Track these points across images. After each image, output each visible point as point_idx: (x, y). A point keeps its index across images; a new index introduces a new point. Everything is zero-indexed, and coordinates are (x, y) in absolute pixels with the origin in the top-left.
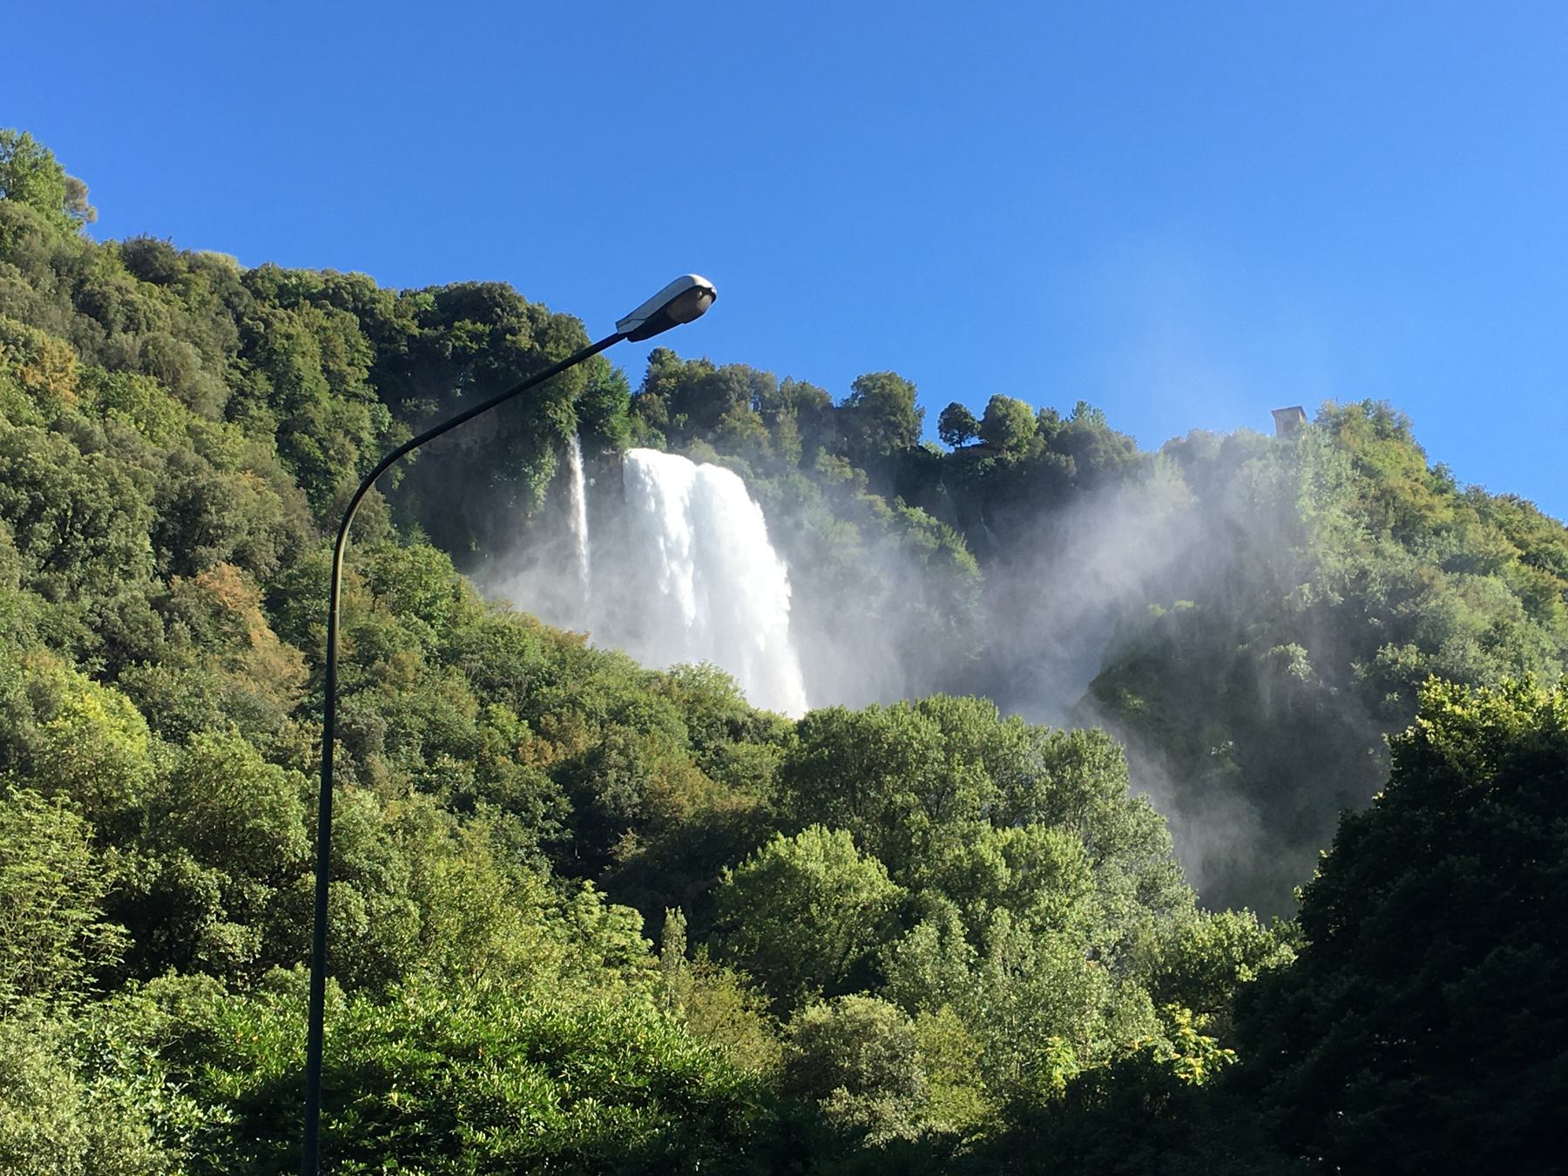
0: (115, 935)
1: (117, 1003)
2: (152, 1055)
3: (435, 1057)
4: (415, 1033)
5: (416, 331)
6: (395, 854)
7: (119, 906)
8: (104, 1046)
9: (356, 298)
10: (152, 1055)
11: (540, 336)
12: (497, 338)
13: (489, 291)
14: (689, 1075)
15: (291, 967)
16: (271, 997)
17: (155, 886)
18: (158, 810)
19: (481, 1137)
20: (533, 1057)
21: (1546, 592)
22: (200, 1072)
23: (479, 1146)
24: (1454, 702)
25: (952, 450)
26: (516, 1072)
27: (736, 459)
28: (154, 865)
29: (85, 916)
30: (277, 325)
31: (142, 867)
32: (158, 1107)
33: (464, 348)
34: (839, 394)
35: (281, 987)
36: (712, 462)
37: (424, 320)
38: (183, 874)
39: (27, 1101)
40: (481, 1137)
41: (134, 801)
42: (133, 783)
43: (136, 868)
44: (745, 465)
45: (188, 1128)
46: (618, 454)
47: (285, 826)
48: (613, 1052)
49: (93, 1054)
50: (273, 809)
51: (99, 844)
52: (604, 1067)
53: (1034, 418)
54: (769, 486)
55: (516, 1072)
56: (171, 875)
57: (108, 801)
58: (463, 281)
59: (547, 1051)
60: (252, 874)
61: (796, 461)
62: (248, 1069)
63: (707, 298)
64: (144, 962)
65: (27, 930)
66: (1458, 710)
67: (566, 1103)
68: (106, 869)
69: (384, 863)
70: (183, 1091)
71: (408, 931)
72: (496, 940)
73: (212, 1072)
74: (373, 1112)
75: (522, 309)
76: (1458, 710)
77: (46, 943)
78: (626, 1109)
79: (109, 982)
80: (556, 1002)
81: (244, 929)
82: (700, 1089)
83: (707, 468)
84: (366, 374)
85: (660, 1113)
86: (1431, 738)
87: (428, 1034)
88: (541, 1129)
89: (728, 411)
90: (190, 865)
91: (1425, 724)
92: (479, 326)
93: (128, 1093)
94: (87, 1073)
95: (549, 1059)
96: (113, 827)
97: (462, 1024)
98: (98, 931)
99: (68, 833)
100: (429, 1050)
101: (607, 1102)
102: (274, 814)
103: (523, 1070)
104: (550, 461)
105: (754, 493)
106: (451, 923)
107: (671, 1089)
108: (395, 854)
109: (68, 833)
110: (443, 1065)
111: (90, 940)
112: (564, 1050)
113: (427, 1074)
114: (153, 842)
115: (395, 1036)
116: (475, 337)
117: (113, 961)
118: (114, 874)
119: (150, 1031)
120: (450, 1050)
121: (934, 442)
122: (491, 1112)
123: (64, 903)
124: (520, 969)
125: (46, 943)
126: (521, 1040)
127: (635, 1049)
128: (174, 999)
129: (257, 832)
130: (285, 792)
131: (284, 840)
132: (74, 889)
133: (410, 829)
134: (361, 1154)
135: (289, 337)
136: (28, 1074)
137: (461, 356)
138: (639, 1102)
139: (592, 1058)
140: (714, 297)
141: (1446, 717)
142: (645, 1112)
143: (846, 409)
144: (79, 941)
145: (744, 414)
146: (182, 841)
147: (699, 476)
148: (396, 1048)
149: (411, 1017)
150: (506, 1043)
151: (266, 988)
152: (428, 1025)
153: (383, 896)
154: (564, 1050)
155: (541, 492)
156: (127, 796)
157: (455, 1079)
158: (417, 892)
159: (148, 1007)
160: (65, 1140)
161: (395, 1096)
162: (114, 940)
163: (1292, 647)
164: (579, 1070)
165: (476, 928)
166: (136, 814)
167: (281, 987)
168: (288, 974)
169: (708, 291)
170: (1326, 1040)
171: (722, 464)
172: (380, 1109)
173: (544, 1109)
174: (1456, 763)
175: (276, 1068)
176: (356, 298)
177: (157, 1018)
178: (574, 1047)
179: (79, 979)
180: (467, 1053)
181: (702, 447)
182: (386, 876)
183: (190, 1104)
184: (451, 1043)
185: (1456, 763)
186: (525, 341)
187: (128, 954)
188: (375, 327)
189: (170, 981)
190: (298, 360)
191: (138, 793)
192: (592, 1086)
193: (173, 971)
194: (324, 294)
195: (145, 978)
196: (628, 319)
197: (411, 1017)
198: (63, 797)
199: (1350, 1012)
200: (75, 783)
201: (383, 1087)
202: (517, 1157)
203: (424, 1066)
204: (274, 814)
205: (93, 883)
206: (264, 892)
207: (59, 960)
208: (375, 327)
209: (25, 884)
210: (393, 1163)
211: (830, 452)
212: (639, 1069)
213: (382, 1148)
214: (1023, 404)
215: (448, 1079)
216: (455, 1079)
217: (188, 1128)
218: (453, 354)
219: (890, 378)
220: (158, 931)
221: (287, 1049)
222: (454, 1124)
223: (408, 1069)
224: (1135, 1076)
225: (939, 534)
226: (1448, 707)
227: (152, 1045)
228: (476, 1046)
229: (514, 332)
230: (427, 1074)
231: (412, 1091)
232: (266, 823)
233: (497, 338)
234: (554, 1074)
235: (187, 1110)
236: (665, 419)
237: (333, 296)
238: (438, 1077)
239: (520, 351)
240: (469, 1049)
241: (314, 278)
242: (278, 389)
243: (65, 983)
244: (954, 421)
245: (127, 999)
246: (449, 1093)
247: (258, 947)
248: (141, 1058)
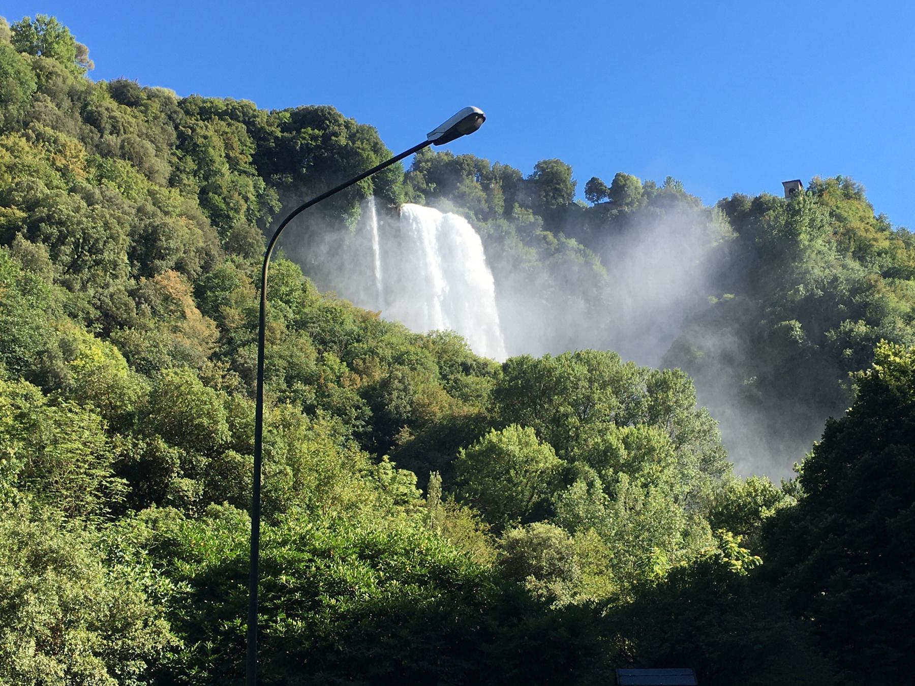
0: (120, 484)
1: (123, 524)
2: (144, 553)
3: (307, 556)
4: (294, 542)
5: (279, 134)
6: (278, 439)
7: (122, 468)
8: (117, 548)
9: (244, 114)
10: (144, 553)
11: (352, 137)
12: (326, 138)
13: (322, 111)
14: (451, 567)
15: (221, 504)
16: (210, 521)
17: (143, 456)
18: (143, 413)
19: (333, 601)
20: (362, 556)
22: (170, 563)
23: (331, 607)
24: (895, 355)
25: (593, 205)
26: (352, 565)
28: (142, 444)
29: (103, 473)
30: (198, 130)
31: (135, 445)
32: (149, 582)
33: (308, 144)
34: (526, 171)
35: (216, 516)
37: (284, 128)
38: (158, 450)
39: (76, 576)
40: (333, 601)
41: (130, 408)
42: (129, 397)
43: (132, 446)
44: (472, 213)
45: (166, 594)
47: (216, 423)
48: (407, 553)
49: (111, 552)
50: (208, 413)
51: (110, 432)
52: (402, 563)
53: (640, 184)
55: (352, 565)
56: (152, 451)
57: (115, 408)
59: (370, 553)
60: (198, 451)
61: (501, 211)
62: (199, 562)
63: (480, 120)
64: (137, 501)
65: (72, 481)
66: (898, 360)
67: (381, 583)
68: (114, 447)
69: (273, 444)
70: (162, 574)
71: (287, 483)
72: (338, 489)
73: (178, 563)
74: (271, 586)
75: (341, 121)
76: (898, 360)
77: (82, 489)
78: (415, 586)
79: (118, 511)
80: (374, 525)
81: (193, 481)
82: (457, 575)
83: (450, 214)
84: (251, 159)
85: (435, 589)
86: (881, 376)
87: (302, 542)
88: (366, 597)
89: (461, 182)
90: (162, 445)
91: (878, 368)
92: (316, 131)
93: (132, 574)
94: (108, 562)
95: (372, 557)
96: (118, 423)
97: (321, 538)
98: (111, 482)
99: (93, 426)
100: (303, 551)
101: (404, 583)
102: (209, 416)
103: (357, 563)
105: (478, 230)
106: (311, 480)
107: (441, 576)
108: (278, 439)
109: (94, 426)
110: (310, 561)
111: (106, 487)
112: (379, 553)
113: (302, 565)
114: (141, 431)
115: (284, 543)
116: (314, 138)
117: (120, 499)
118: (119, 449)
119: (142, 540)
120: (314, 552)
121: (581, 200)
122: (338, 587)
123: (92, 466)
124: (351, 506)
125: (82, 489)
126: (355, 546)
127: (420, 552)
128: (155, 521)
129: (200, 425)
130: (216, 403)
131: (215, 431)
132: (97, 458)
133: (287, 425)
134: (265, 611)
135: (205, 137)
136: (79, 561)
137: (306, 149)
138: (422, 583)
139: (395, 557)
140: (484, 119)
141: (890, 364)
142: (426, 589)
143: (531, 181)
144: (101, 488)
146: (158, 430)
148: (284, 550)
149: (292, 533)
150: (346, 548)
151: (207, 515)
152: (302, 538)
153: (272, 464)
154: (379, 553)
156: (125, 405)
157: (318, 568)
158: (293, 462)
159: (139, 526)
160: (99, 599)
161: (284, 578)
162: (120, 487)
163: (793, 322)
164: (388, 564)
165: (326, 482)
166: (131, 415)
167: (216, 516)
168: (219, 508)
169: (481, 116)
170: (817, 551)
172: (275, 585)
173: (368, 586)
174: (895, 390)
175: (215, 561)
176: (244, 114)
177: (146, 532)
178: (384, 551)
179: (101, 509)
180: (325, 554)
181: (446, 202)
182: (273, 453)
183: (167, 581)
184: (315, 548)
185: (895, 390)
186: (343, 141)
187: (129, 496)
188: (256, 133)
189: (152, 511)
190: (210, 150)
191: (131, 402)
192: (396, 573)
193: (154, 505)
194: (226, 112)
195: (138, 509)
196: (434, 133)
197: (292, 533)
198: (90, 405)
199: (831, 535)
200: (95, 397)
201: (277, 572)
202: (353, 613)
203: (300, 561)
204: (209, 416)
205: (108, 454)
206: (204, 461)
207: (89, 498)
208: (256, 133)
209: (69, 455)
210: (283, 615)
211: (521, 206)
212: (421, 564)
213: (277, 607)
214: (635, 178)
215: (314, 568)
216: (318, 568)
217: (166, 594)
218: (301, 148)
219: (556, 162)
220: (145, 483)
221: (220, 550)
222: (317, 594)
223: (291, 563)
224: (708, 571)
225: (585, 256)
226: (892, 358)
227: (144, 547)
228: (329, 550)
229: (336, 134)
230: (302, 565)
231: (293, 575)
232: (205, 421)
233: (326, 138)
234: (374, 566)
235: (165, 584)
236: (425, 186)
237: (230, 114)
238: (308, 567)
240: (325, 552)
241: (220, 103)
242: (199, 168)
243: (92, 511)
244: (594, 188)
245: (128, 520)
246: (315, 576)
247: (202, 492)
248: (137, 554)
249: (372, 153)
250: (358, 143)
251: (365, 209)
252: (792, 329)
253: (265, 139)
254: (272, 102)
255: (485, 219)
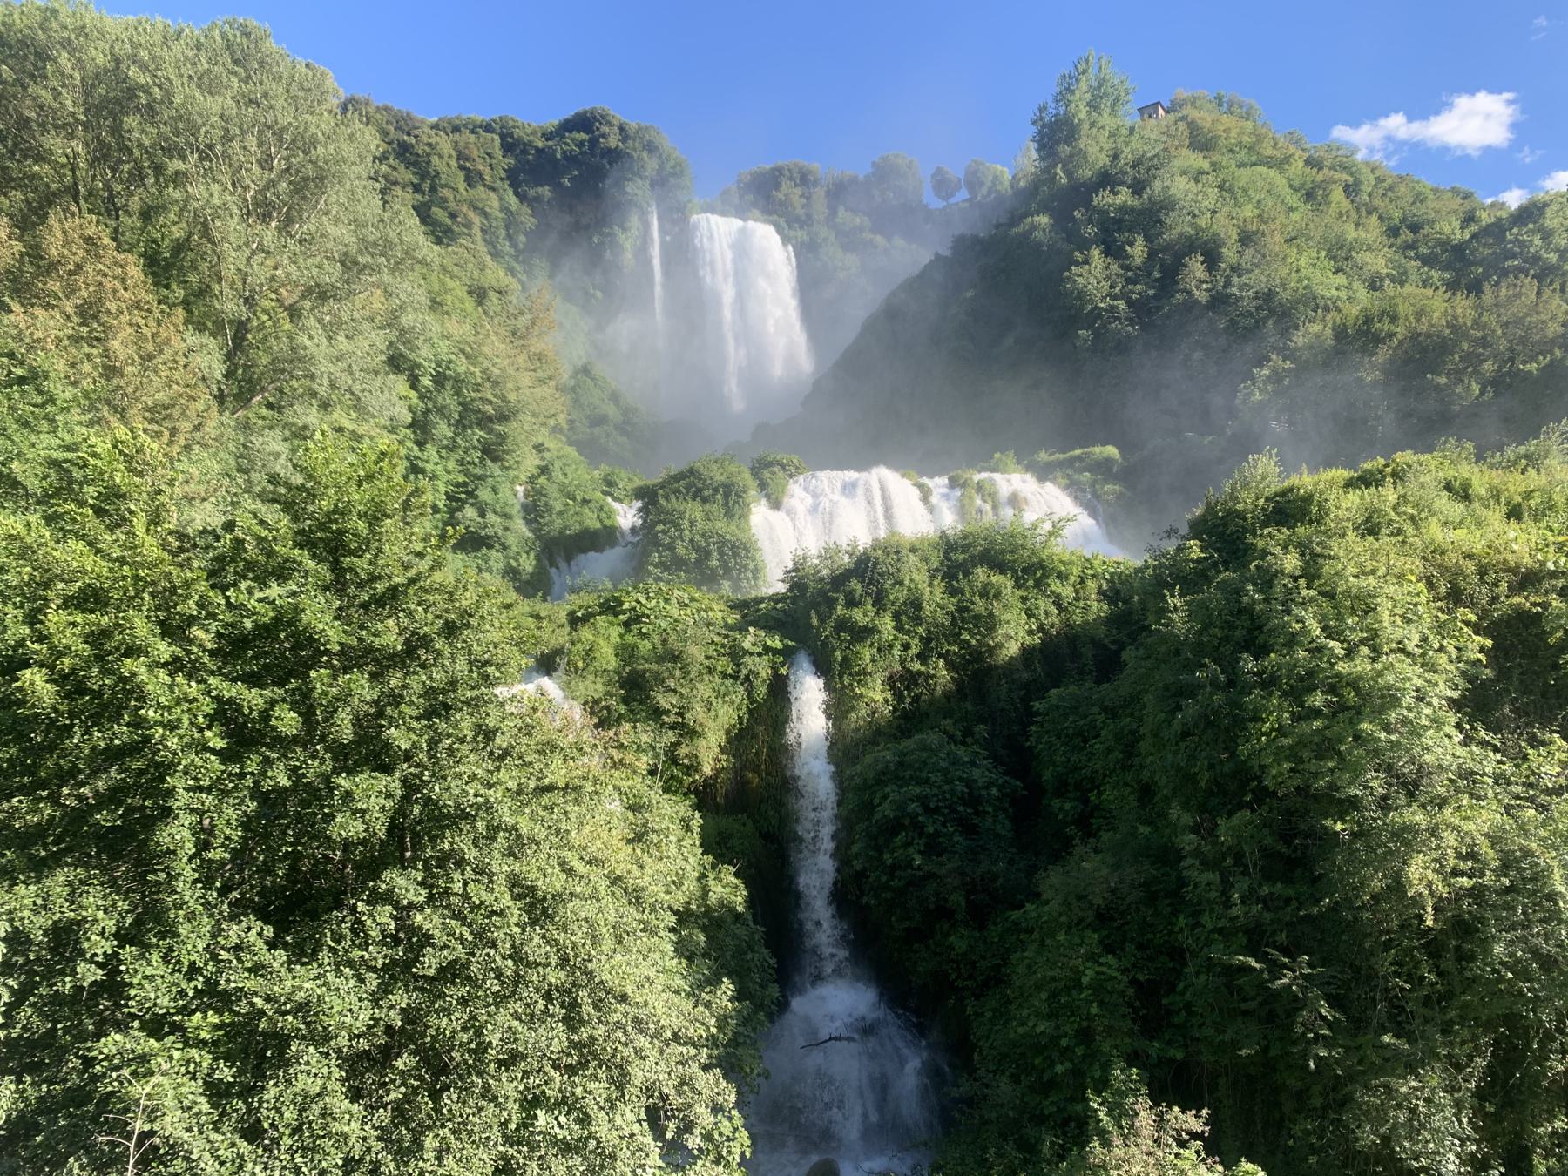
5: (540, 145)
11: (624, 140)
12: (594, 142)
21: (1325, 185)
27: (775, 217)
36: (755, 220)
37: (548, 136)
44: (782, 221)
46: (685, 219)
54: (801, 234)
58: (580, 109)
75: (616, 122)
83: (751, 224)
84: (503, 174)
92: (583, 136)
104: (634, 221)
105: (785, 240)
116: (581, 144)
135: (430, 145)
137: (569, 158)
145: (790, 192)
147: (743, 232)
155: (628, 245)
171: (765, 221)
190: (435, 160)
229: (604, 136)
237: (488, 128)
239: (609, 150)
241: (478, 118)
242: (423, 176)
244: (942, 185)
249: (645, 155)
250: (630, 143)
251: (646, 226)
252: (1034, 227)
253: (525, 152)
254: (538, 114)
255: (801, 228)
